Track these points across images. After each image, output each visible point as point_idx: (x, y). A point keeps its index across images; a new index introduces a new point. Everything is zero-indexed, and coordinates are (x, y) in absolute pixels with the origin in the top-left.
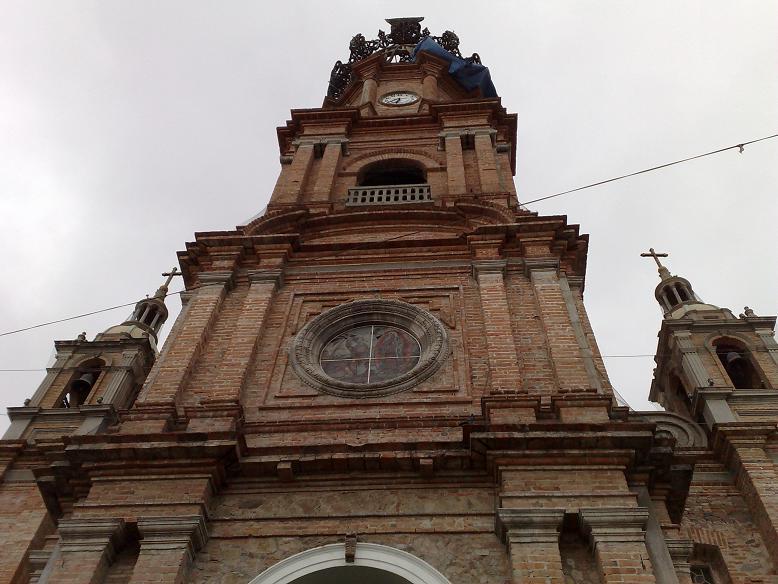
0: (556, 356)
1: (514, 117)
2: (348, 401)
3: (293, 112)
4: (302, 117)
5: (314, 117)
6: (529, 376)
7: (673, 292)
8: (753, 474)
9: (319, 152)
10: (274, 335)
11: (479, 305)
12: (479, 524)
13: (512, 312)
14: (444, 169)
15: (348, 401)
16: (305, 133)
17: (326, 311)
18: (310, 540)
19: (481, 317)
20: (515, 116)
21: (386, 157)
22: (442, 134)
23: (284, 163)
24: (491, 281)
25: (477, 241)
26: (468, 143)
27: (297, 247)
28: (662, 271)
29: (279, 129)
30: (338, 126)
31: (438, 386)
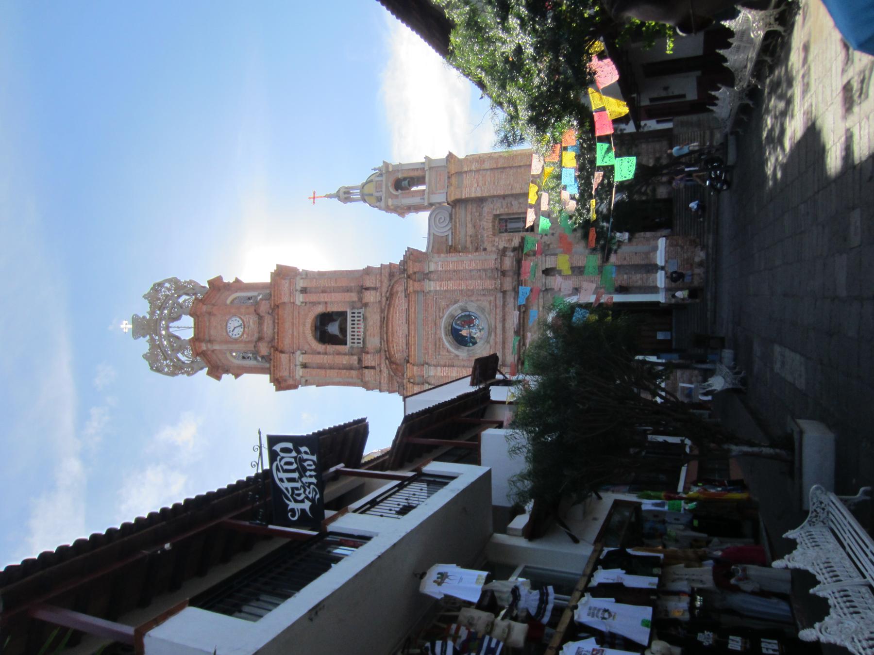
0: (479, 268)
1: (278, 266)
2: (493, 334)
6: (484, 276)
7: (345, 195)
8: (468, 196)
9: (305, 366)
10: (456, 363)
11: (446, 291)
12: (541, 294)
13: (450, 279)
14: (326, 303)
15: (493, 334)
16: (285, 374)
17: (447, 344)
19: (454, 291)
20: (278, 266)
22: (298, 303)
23: (307, 383)
24: (432, 286)
25: (411, 289)
26: (304, 291)
27: (408, 362)
28: (330, 196)
31: (488, 305)
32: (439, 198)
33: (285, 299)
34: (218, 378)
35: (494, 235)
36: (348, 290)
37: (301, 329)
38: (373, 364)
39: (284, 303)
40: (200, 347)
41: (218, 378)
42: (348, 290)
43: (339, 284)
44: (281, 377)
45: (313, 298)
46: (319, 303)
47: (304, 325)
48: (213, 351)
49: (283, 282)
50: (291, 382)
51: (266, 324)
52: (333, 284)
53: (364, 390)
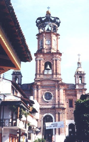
16: (38, 56)
17: (45, 93)
18: (46, 113)
20: (62, 53)
21: (47, 61)
29: (34, 54)
32: (77, 87)
33: (54, 56)
34: (36, 35)
35: (69, 99)
36: (56, 71)
38: (41, 77)
41: (36, 35)
42: (56, 71)
43: (57, 68)
45: (54, 61)
46: (53, 63)
47: (48, 60)
49: (58, 55)
52: (57, 67)
53: (35, 74)
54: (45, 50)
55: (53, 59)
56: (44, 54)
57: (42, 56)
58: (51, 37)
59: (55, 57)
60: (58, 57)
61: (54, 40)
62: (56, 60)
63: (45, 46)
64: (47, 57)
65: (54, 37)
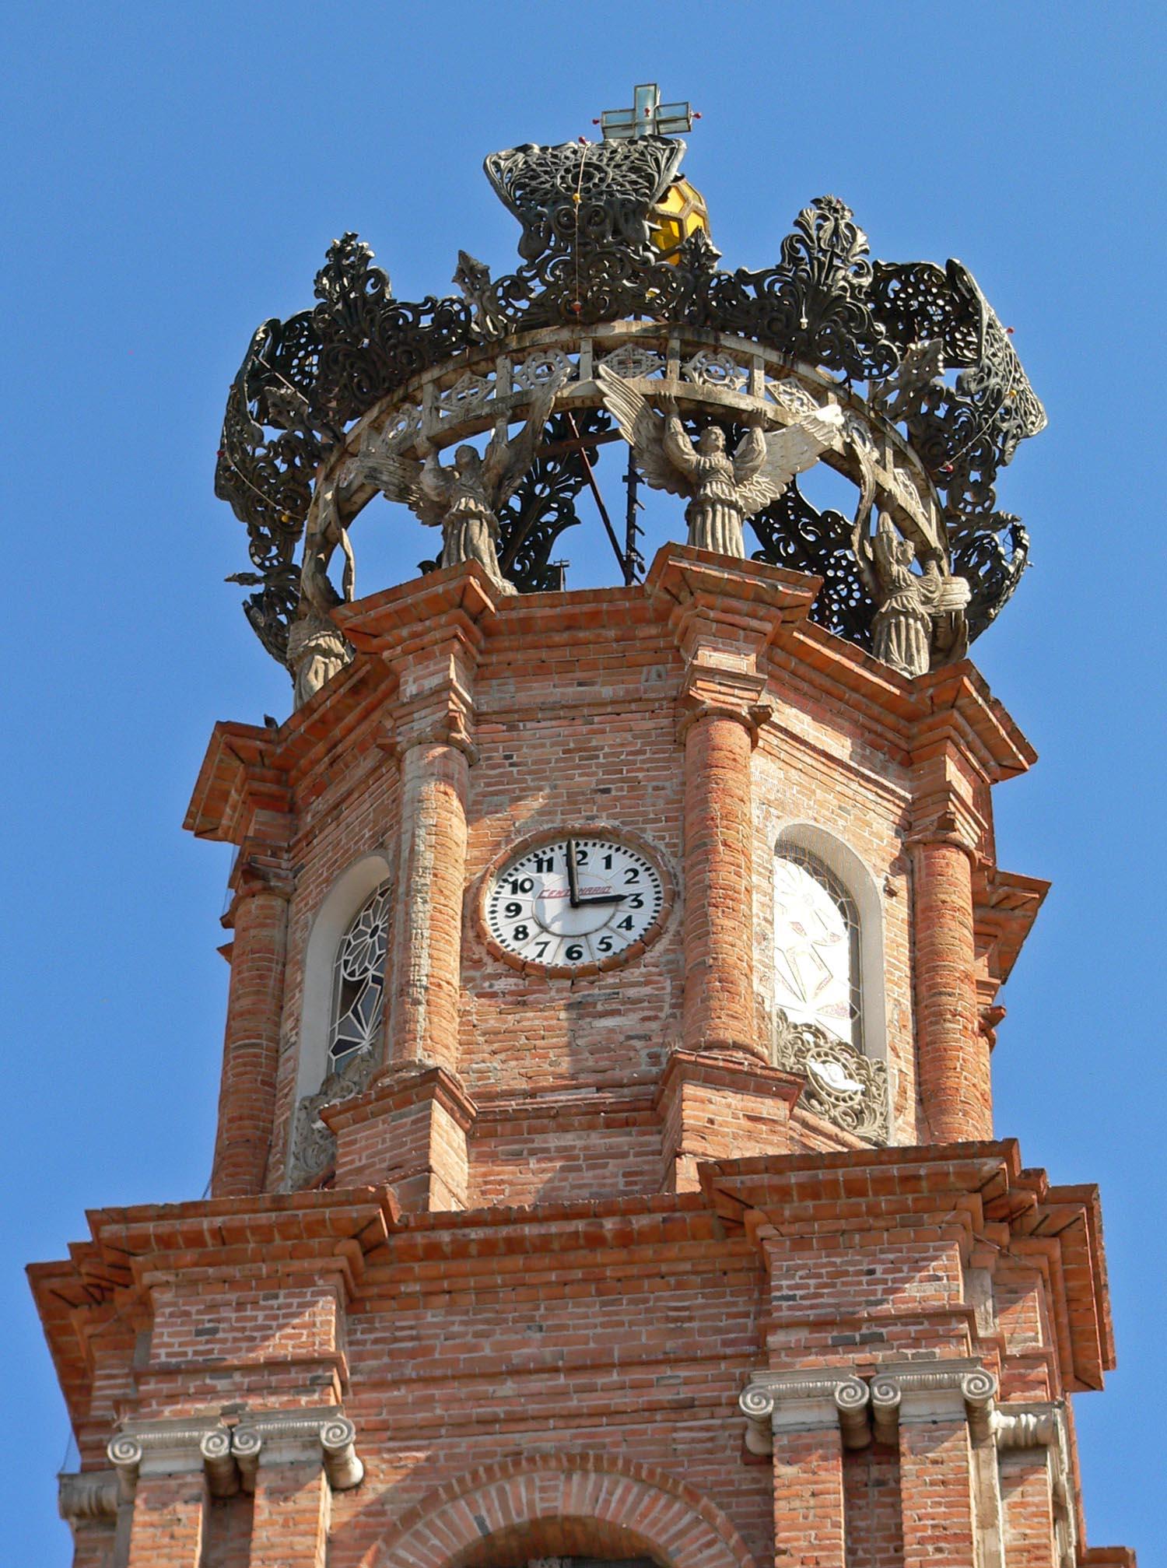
1: (1085, 1195)
3: (96, 1219)
4: (141, 1244)
5: (195, 1240)
16: (169, 1341)
20: (1085, 1195)
29: (38, 1274)
30: (304, 1281)
37: (549, 1439)
39: (762, 1275)
40: (423, 653)
44: (145, 1306)
47: (575, 1463)
48: (392, 754)
50: (106, 1387)
51: (598, 1140)
54: (443, 1123)
55: (751, 1404)
56: (384, 1256)
57: (318, 1324)
58: (687, 720)
59: (840, 1328)
60: (939, 1321)
61: (792, 849)
62: (869, 1445)
63: (443, 1031)
64: (531, 1348)
65: (794, 787)
